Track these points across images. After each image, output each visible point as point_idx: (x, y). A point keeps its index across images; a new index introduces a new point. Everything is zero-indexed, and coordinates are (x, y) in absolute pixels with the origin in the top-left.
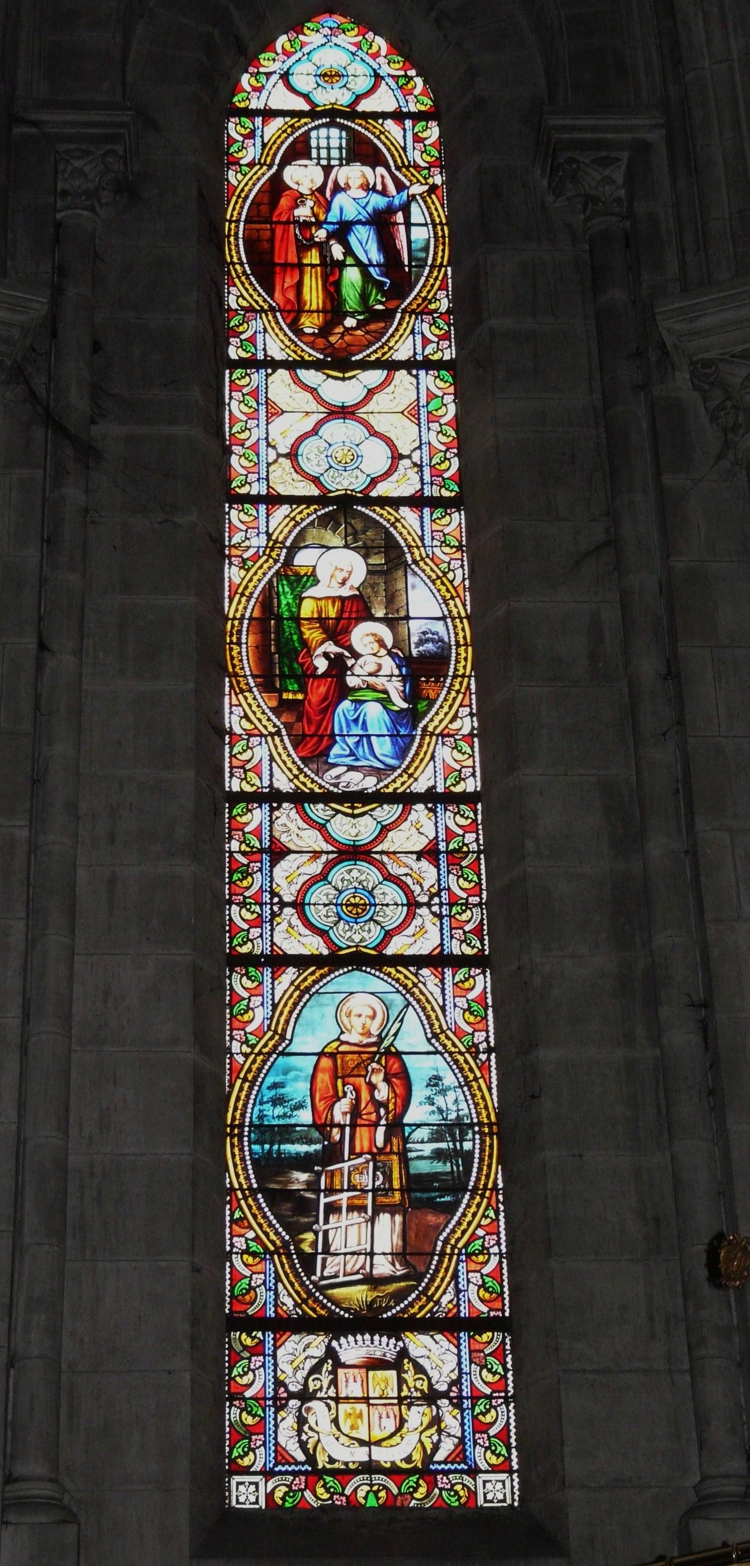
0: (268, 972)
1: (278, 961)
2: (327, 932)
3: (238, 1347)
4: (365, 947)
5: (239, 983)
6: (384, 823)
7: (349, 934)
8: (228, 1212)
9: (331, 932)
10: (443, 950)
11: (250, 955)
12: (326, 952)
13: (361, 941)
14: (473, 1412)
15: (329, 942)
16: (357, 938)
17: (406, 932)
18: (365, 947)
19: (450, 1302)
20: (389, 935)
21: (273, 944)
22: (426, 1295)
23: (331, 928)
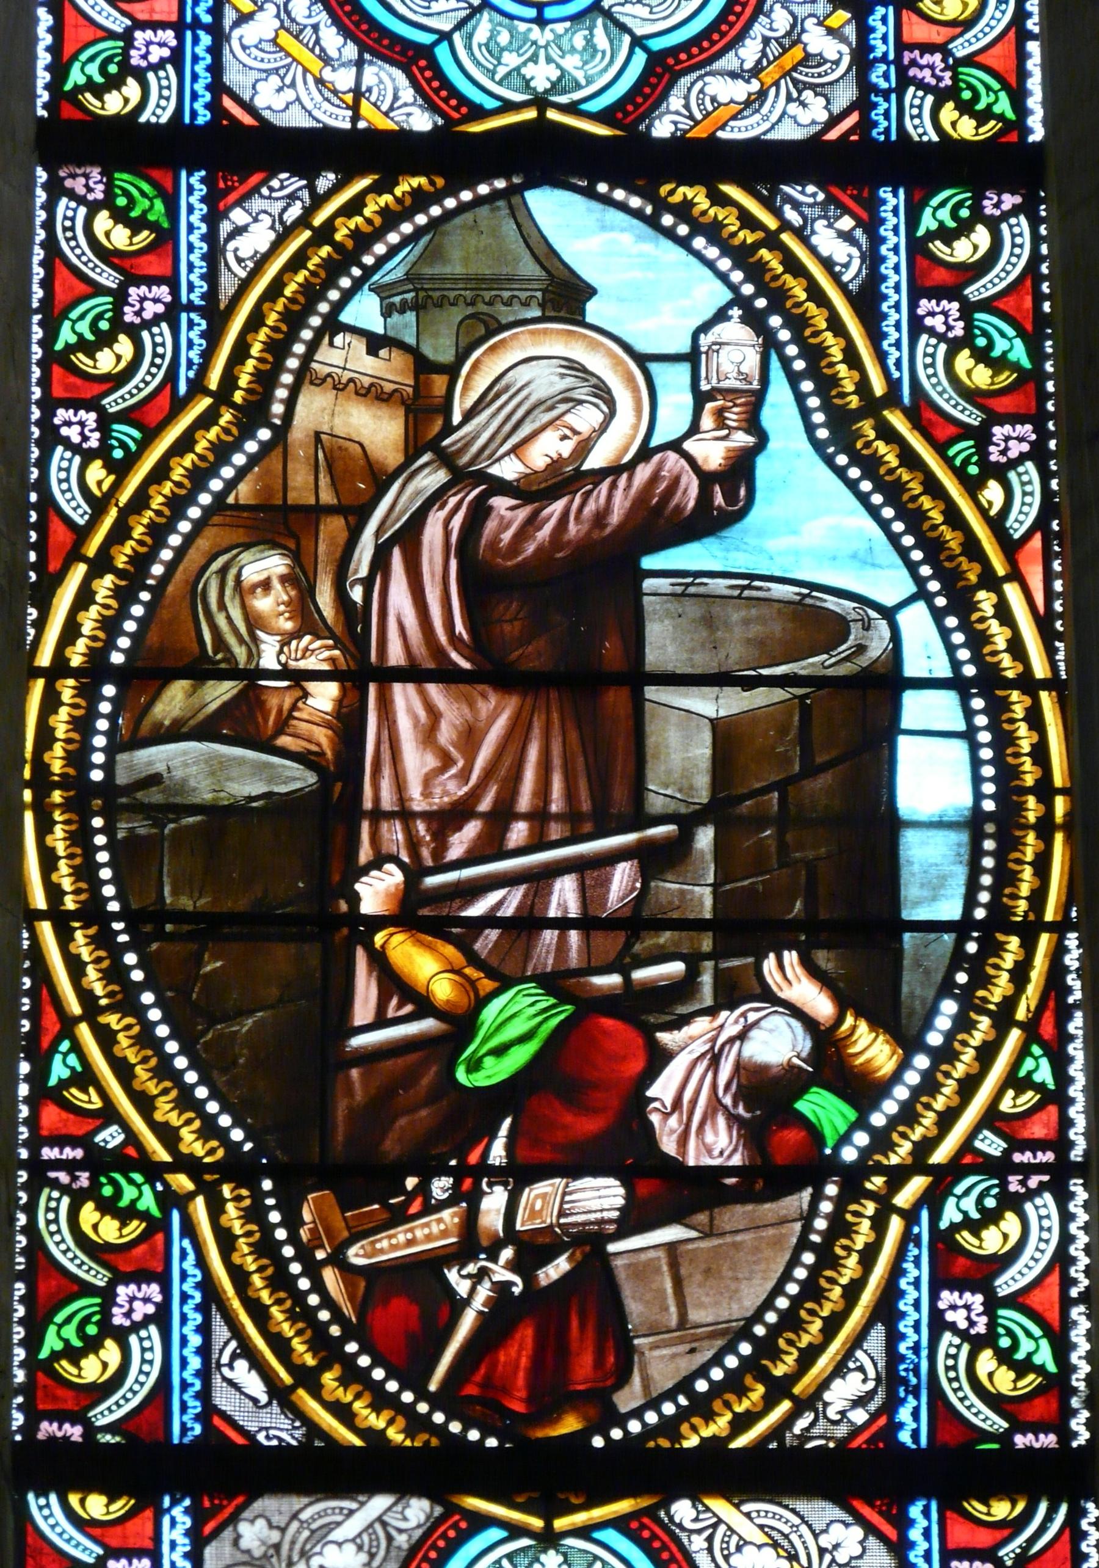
0: (193, 187)
1: (237, 150)
2: (427, 52)
3: (78, 253)
4: (571, 109)
5: (84, 223)
6: (656, 45)
7: (511, 60)
8: (37, 333)
9: (442, 53)
10: (866, 124)
11: (127, 122)
12: (422, 122)
13: (556, 87)
14: (935, 1216)
15: (432, 86)
16: (541, 76)
17: (729, 61)
18: (571, 109)
19: (859, 1402)
20: (664, 70)
21: (218, 87)
22: (764, 1376)
23: (445, 36)
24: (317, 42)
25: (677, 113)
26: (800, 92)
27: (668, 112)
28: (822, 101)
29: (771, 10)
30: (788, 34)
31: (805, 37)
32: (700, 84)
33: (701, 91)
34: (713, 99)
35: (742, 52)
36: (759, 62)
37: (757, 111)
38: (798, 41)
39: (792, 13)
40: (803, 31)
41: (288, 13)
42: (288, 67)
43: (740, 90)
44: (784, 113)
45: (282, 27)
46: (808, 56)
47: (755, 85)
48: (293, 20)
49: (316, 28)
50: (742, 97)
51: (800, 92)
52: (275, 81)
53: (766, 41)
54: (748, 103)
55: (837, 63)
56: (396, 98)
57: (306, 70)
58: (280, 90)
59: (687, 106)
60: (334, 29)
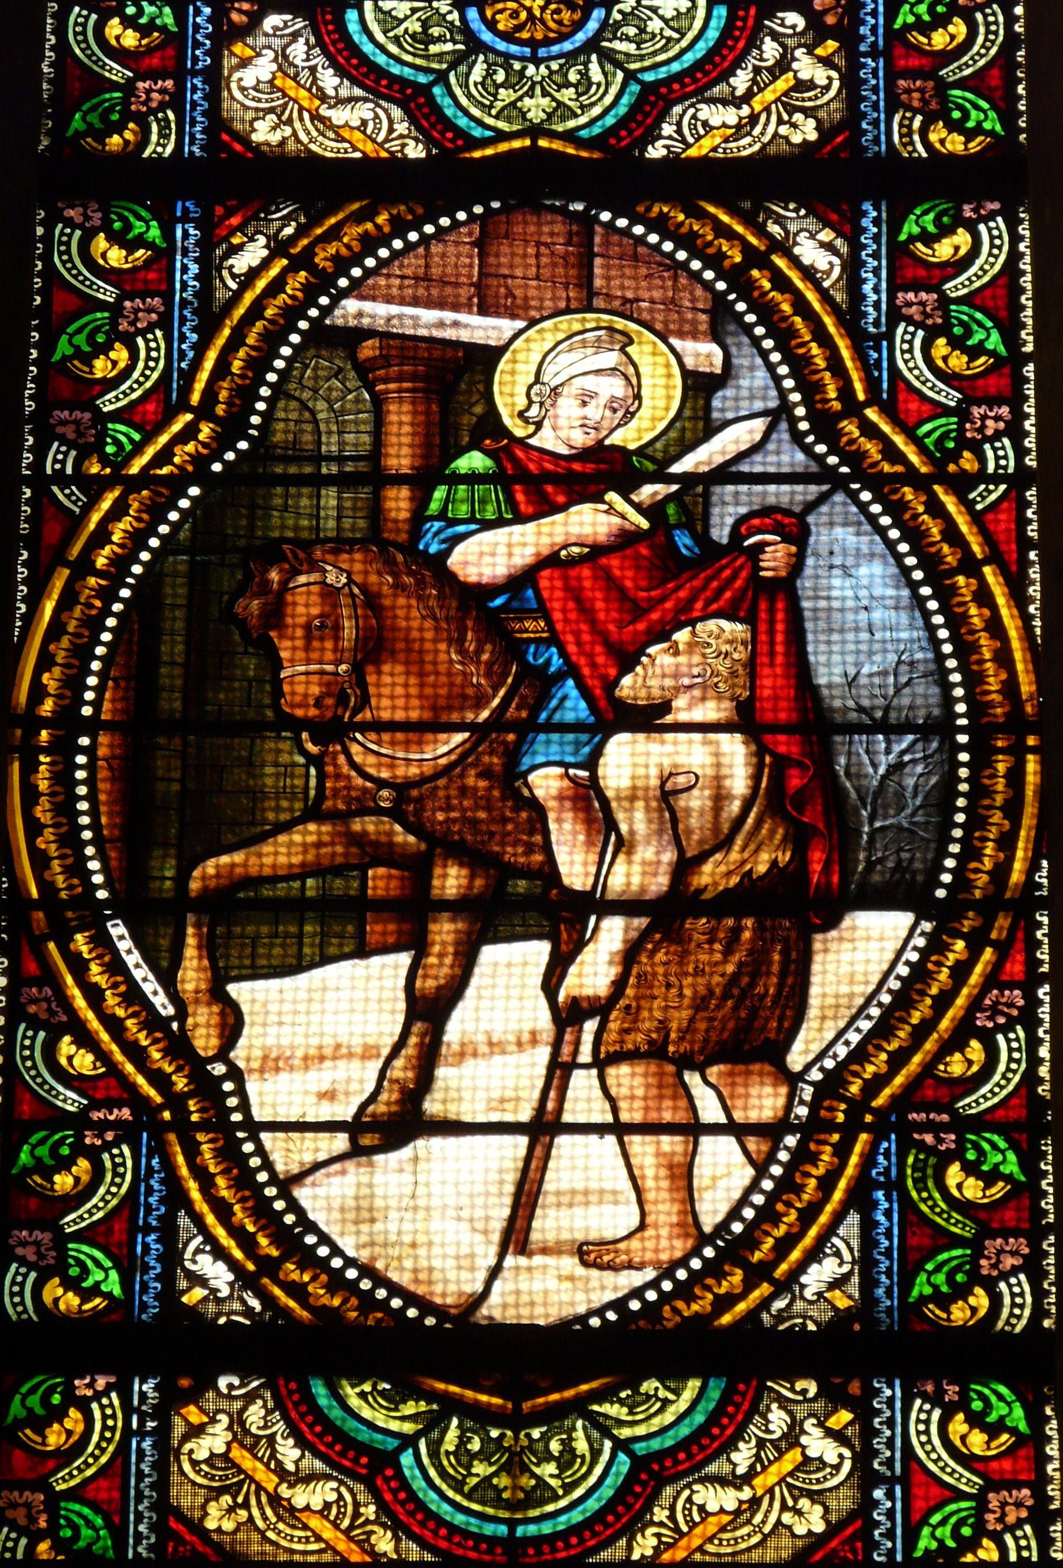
24: (273, 1456)
25: (661, 1524)
26: (796, 1500)
27: (652, 1523)
28: (818, 1510)
29: (769, 1409)
30: (784, 1436)
31: (804, 1440)
32: (686, 1493)
33: (689, 1500)
34: (702, 1508)
35: (735, 1456)
36: (752, 1467)
37: (749, 1522)
38: (796, 1444)
39: (790, 1413)
40: (803, 1432)
41: (242, 1423)
42: (241, 1483)
43: (730, 1499)
44: (779, 1522)
45: (235, 1438)
46: (807, 1460)
47: (746, 1494)
48: (247, 1432)
49: (271, 1439)
50: (731, 1506)
51: (796, 1500)
52: (226, 1500)
53: (761, 1444)
54: (737, 1513)
55: (837, 1468)
56: (356, 1515)
57: (260, 1488)
58: (231, 1510)
59: (672, 1517)
60: (291, 1442)
